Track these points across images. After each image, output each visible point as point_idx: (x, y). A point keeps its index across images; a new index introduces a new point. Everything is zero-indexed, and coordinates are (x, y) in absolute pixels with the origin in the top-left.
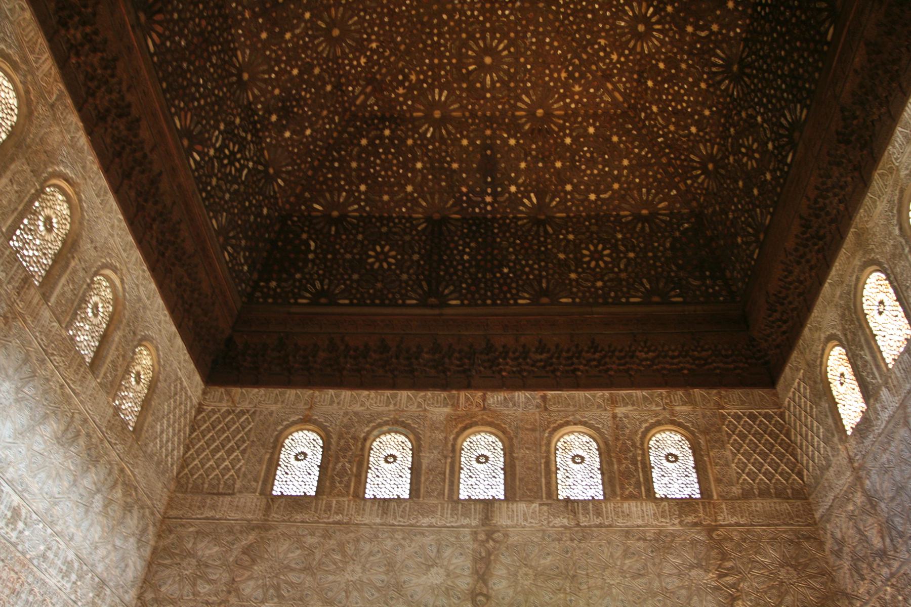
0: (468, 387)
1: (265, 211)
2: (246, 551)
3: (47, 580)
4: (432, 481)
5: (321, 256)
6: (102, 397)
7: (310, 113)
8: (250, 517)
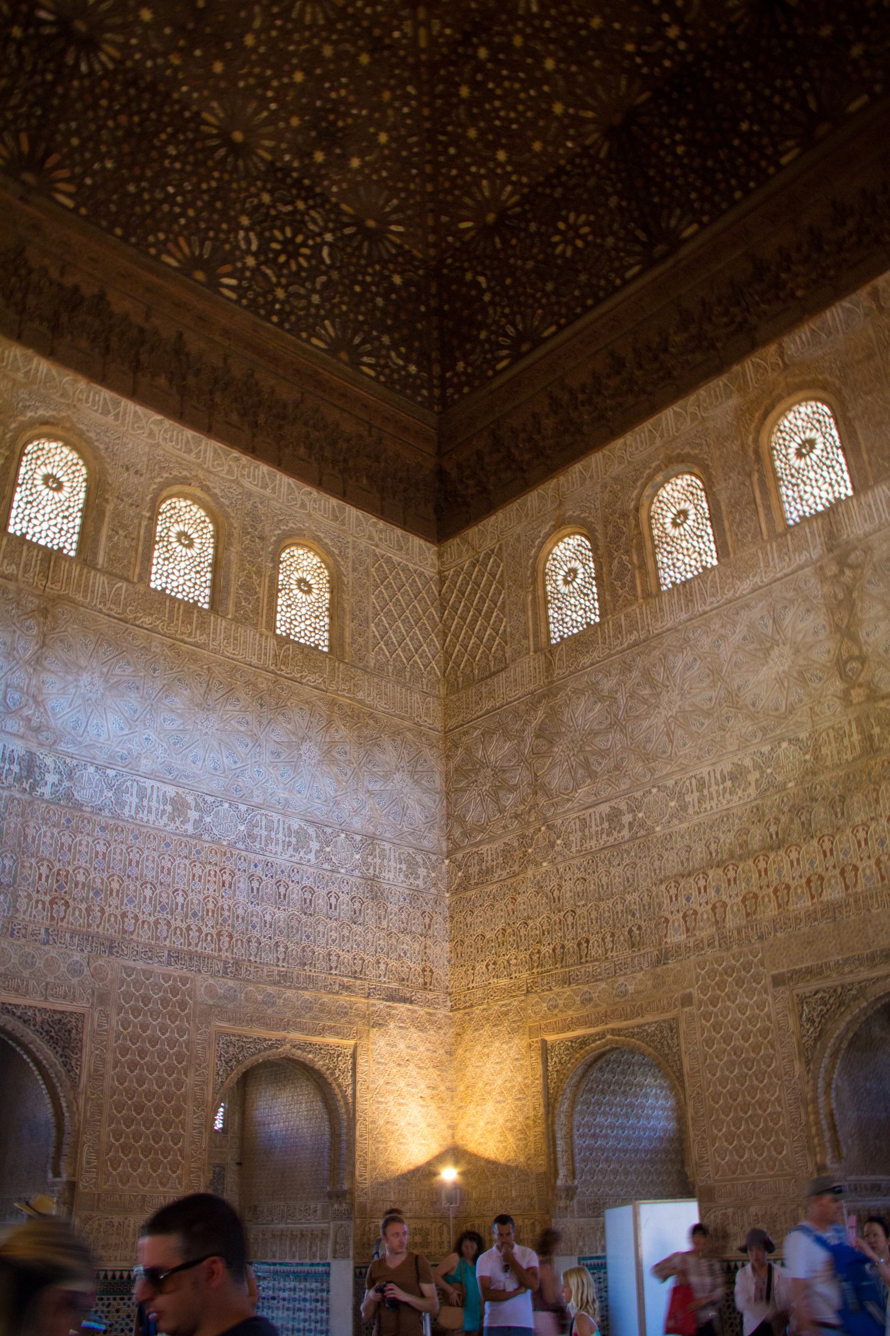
0: (754, 346)
1: (397, 280)
2: (540, 734)
3: (270, 860)
4: (741, 521)
5: (498, 288)
6: (247, 634)
7: (364, 112)
8: (532, 687)
